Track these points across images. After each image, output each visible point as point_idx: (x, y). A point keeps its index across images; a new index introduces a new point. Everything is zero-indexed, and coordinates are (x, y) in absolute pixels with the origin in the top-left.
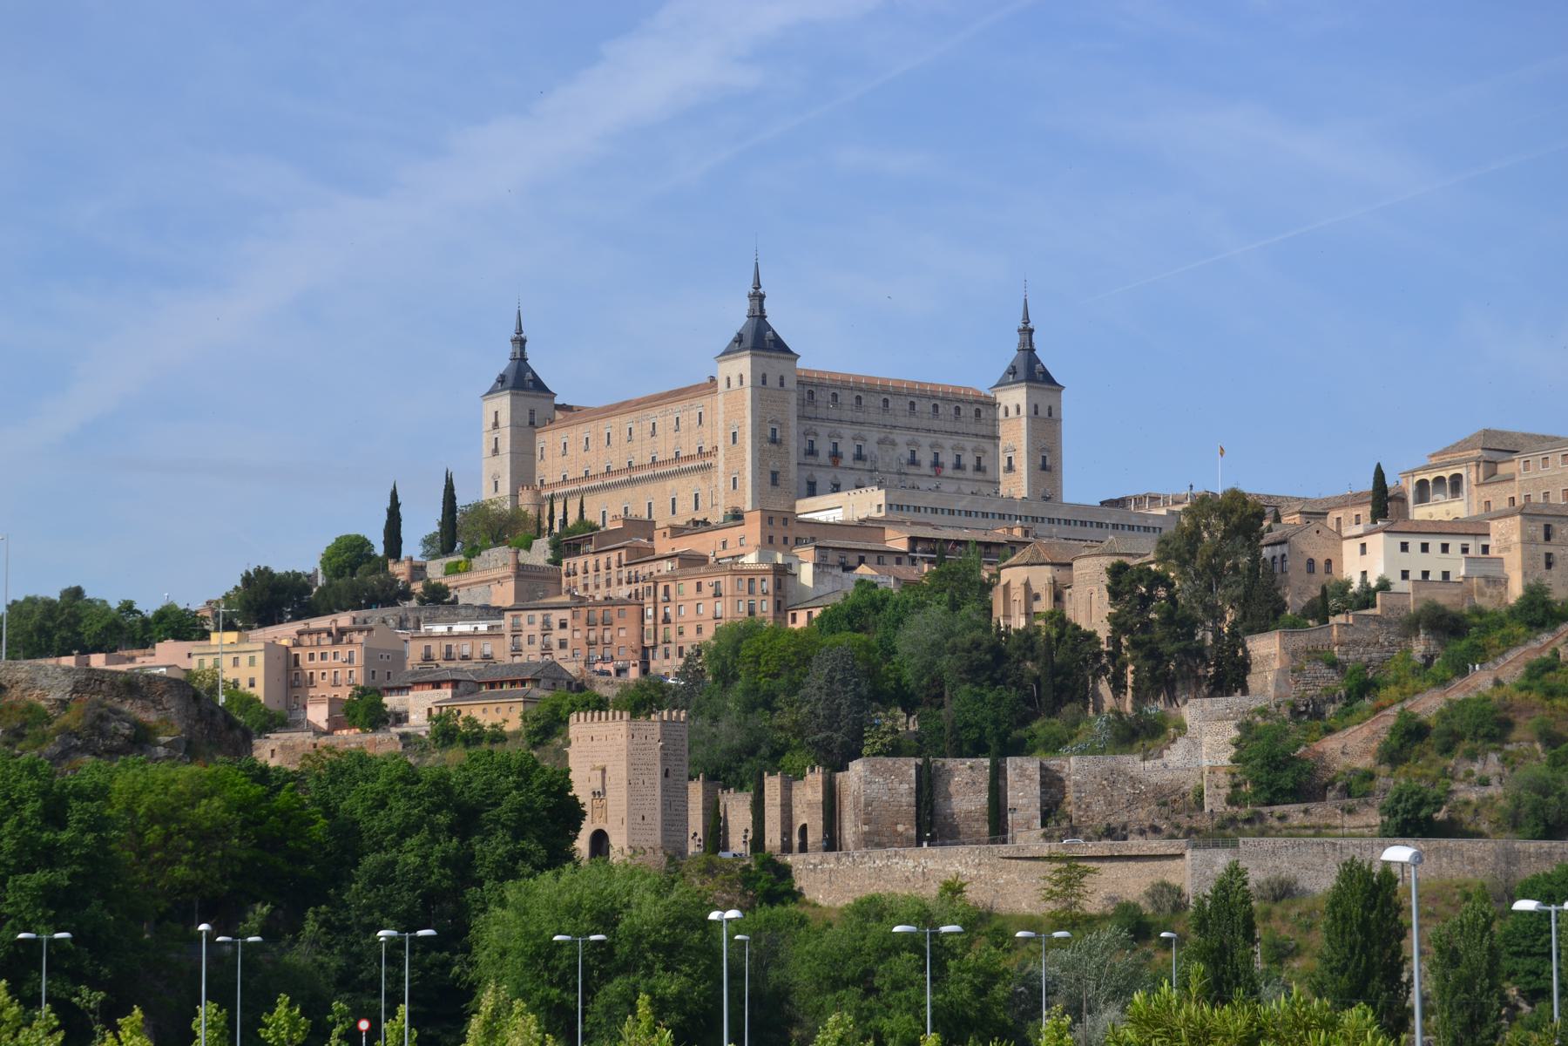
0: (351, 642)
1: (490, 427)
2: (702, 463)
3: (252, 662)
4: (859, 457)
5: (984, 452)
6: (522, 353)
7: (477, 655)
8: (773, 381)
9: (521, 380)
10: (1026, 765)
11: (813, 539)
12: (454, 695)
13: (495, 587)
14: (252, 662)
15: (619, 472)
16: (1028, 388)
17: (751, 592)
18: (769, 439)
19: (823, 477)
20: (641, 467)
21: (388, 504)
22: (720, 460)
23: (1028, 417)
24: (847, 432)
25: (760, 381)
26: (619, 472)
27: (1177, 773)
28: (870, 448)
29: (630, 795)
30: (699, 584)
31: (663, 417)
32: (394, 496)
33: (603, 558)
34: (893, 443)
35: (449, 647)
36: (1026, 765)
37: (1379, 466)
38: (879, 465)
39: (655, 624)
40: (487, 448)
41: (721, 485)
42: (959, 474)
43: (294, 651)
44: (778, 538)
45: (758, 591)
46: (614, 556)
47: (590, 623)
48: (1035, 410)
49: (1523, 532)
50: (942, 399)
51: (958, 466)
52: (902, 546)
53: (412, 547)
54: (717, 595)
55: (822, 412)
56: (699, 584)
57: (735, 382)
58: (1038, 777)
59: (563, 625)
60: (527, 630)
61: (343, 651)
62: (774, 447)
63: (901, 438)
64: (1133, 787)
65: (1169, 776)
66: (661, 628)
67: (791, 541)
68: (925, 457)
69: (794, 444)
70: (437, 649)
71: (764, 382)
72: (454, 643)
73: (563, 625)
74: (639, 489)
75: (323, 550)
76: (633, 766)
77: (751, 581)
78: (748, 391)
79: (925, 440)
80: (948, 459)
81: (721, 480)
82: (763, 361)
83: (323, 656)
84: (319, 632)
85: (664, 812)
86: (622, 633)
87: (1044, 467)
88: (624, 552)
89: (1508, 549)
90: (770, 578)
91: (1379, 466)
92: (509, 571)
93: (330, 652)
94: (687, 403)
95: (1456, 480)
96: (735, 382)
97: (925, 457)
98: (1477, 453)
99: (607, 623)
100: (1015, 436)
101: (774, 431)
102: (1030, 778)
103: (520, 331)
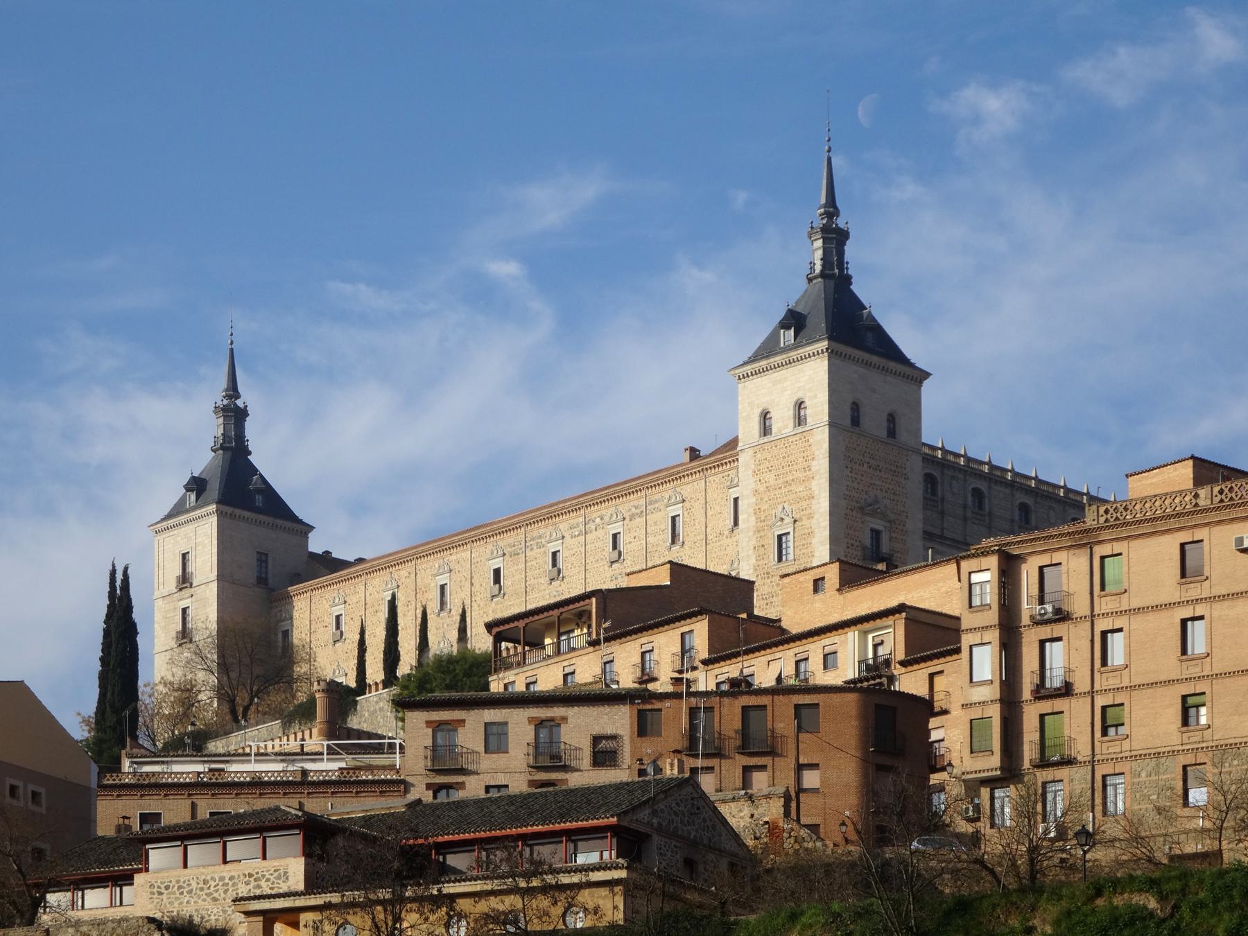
1: (172, 585)
8: (874, 423)
25: (848, 420)
46: (664, 646)
57: (782, 421)
66: (1030, 714)
71: (856, 421)
78: (820, 439)
96: (782, 421)
101: (876, 534)
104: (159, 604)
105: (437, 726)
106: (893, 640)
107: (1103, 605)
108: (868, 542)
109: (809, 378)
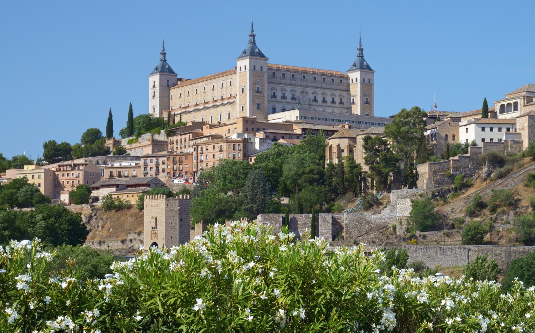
0: (79, 170)
1: (152, 87)
2: (230, 101)
4: (293, 98)
5: (343, 96)
6: (164, 58)
7: (130, 175)
8: (258, 68)
10: (326, 216)
11: (264, 129)
12: (117, 190)
13: (145, 149)
15: (200, 104)
16: (361, 71)
17: (234, 149)
18: (256, 92)
19: (278, 106)
20: (208, 102)
21: (108, 116)
22: (237, 100)
23: (361, 83)
24: (288, 88)
25: (253, 69)
26: (200, 104)
27: (386, 220)
28: (298, 94)
29: (166, 228)
30: (214, 146)
31: (217, 83)
33: (183, 137)
34: (307, 93)
35: (120, 172)
36: (326, 216)
37: (485, 99)
38: (301, 101)
39: (197, 162)
40: (151, 96)
41: (238, 109)
42: (333, 105)
43: (56, 173)
44: (250, 129)
45: (237, 148)
46: (187, 136)
47: (174, 163)
48: (363, 81)
49: (529, 123)
50: (327, 76)
51: (333, 102)
52: (299, 132)
53: (116, 135)
54: (221, 151)
55: (278, 80)
56: (214, 146)
58: (331, 221)
59: (163, 163)
60: (150, 165)
61: (75, 173)
62: (258, 94)
63: (310, 91)
64: (368, 225)
65: (383, 221)
66: (199, 164)
67: (255, 130)
68: (320, 99)
69: (266, 93)
70: (115, 172)
72: (121, 170)
73: (163, 163)
74: (208, 111)
75: (82, 134)
76: (167, 217)
77: (234, 145)
78: (248, 72)
79: (320, 92)
80: (329, 99)
81: (238, 107)
82: (254, 60)
83: (68, 175)
84: (67, 165)
85: (180, 235)
86: (187, 166)
87: (367, 103)
88: (191, 134)
89: (523, 129)
90: (241, 144)
91: (485, 99)
92: (149, 142)
93: (70, 173)
94: (225, 77)
95: (516, 104)
97: (320, 99)
98: (524, 93)
99: (181, 163)
100: (356, 91)
101: (258, 88)
102: (327, 222)
103: (164, 50)
104: (150, 90)
105: (145, 160)
107: (207, 152)
108: (256, 89)
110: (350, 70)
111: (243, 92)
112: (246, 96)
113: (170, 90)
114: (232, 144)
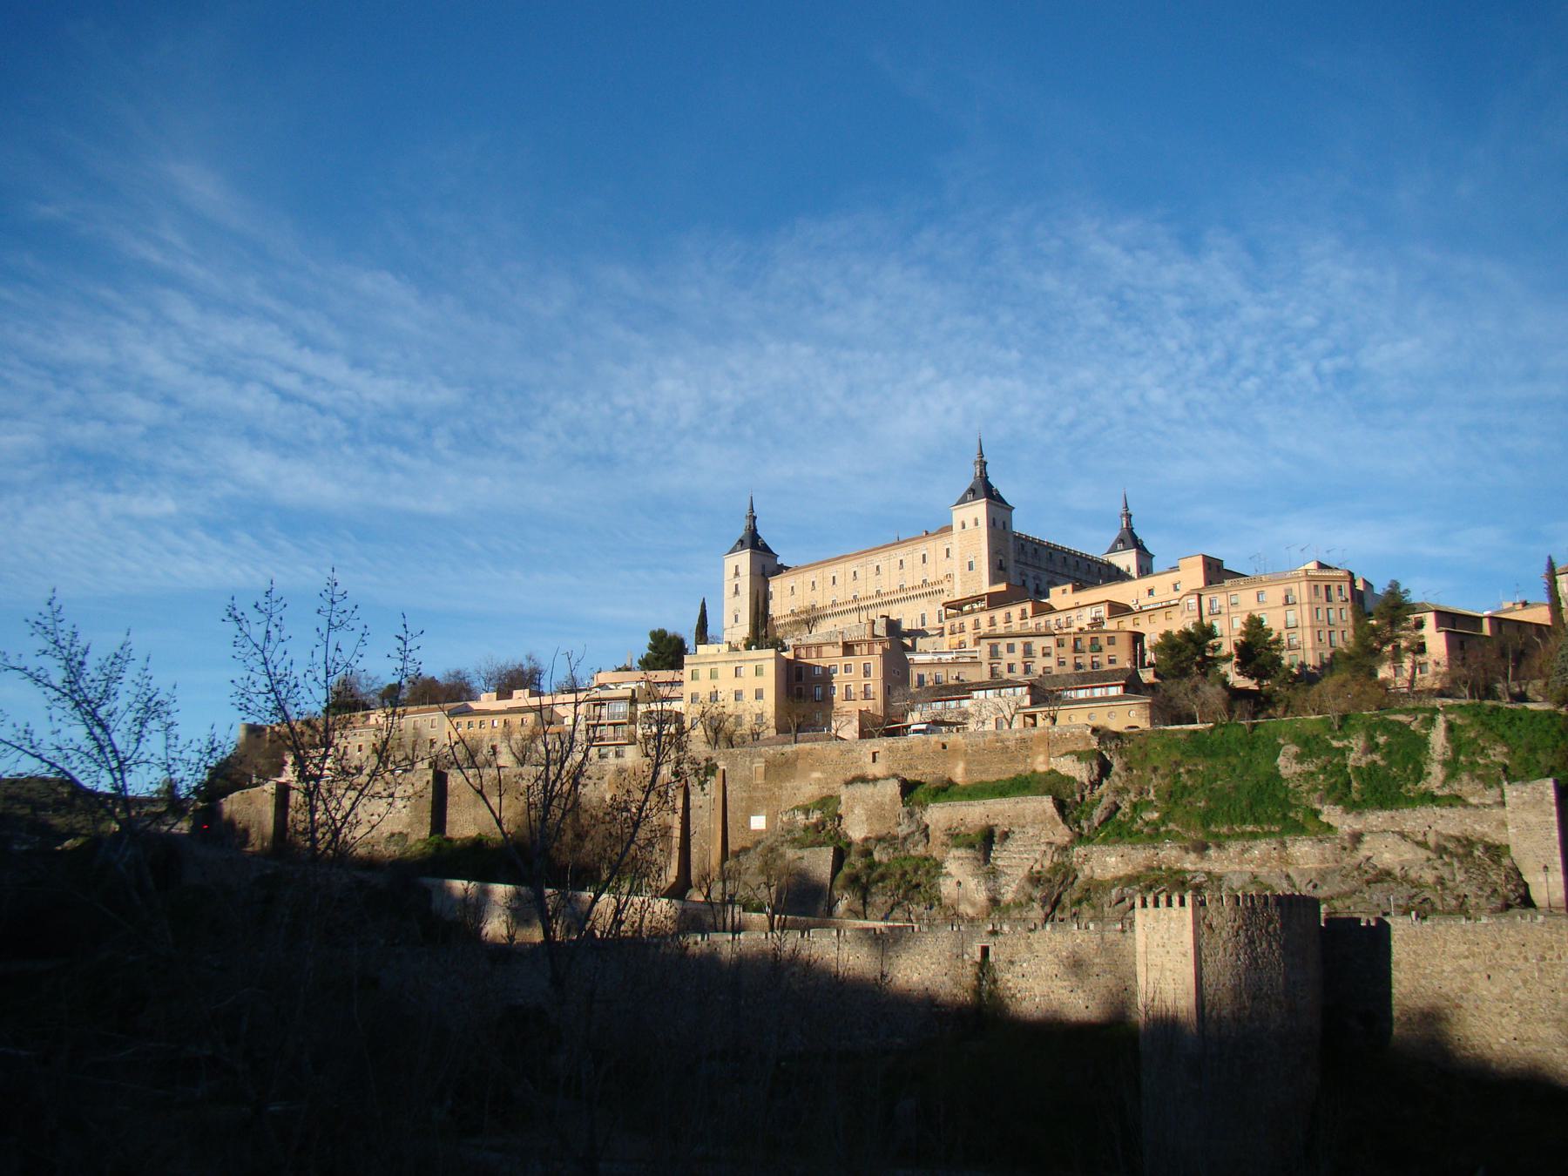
3: (758, 672)
8: (1000, 525)
9: (753, 542)
14: (759, 671)
17: (1329, 599)
25: (992, 523)
32: (703, 605)
57: (970, 524)
77: (1328, 588)
96: (970, 524)
106: (1103, 611)
109: (979, 509)
110: (1113, 550)
111: (971, 568)
112: (980, 574)
113: (767, 583)
114: (1322, 586)
